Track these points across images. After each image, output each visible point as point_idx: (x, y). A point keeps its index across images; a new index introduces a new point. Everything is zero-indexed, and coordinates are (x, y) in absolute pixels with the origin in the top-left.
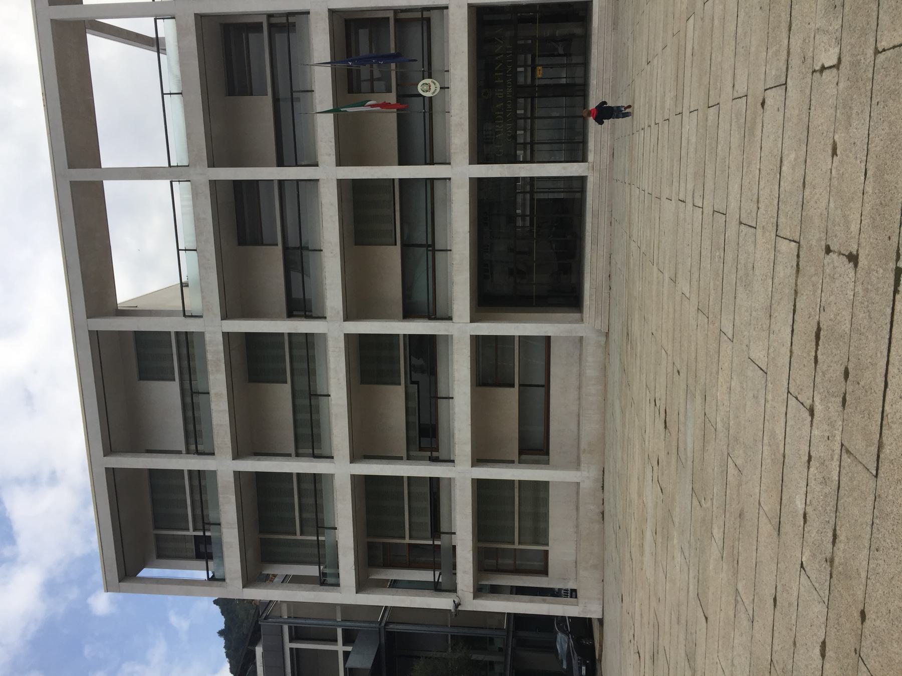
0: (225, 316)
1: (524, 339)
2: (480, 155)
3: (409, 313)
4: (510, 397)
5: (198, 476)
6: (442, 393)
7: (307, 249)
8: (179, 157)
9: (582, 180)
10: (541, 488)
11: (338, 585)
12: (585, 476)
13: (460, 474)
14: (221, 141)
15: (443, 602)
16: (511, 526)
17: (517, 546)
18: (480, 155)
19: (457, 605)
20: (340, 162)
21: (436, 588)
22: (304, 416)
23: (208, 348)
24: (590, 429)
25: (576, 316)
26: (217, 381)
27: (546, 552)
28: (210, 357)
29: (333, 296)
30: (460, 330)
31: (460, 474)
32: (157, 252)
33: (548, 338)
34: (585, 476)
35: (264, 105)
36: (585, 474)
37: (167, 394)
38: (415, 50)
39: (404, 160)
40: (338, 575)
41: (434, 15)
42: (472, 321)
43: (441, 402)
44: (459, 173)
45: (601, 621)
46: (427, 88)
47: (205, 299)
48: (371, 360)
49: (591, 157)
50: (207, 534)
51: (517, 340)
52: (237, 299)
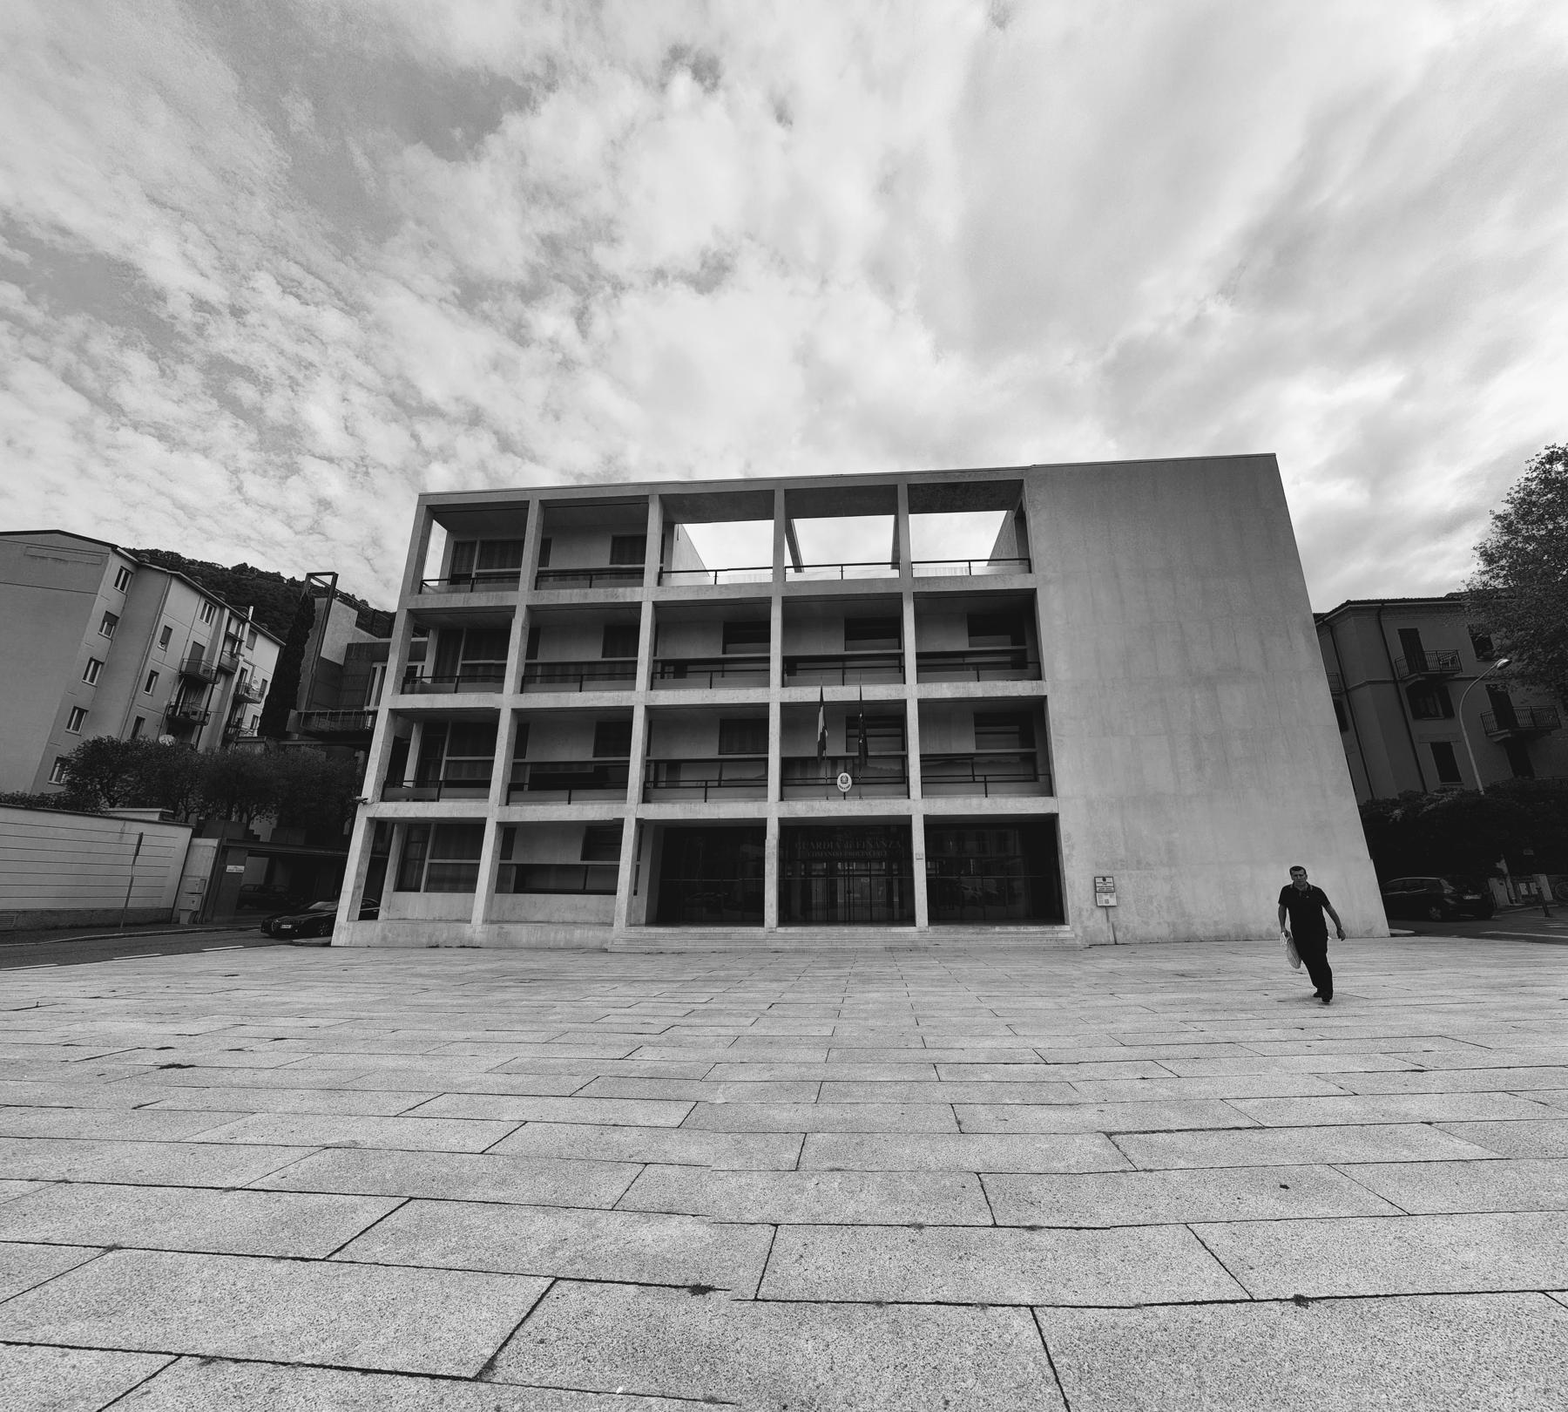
0: (656, 605)
1: (615, 871)
2: (787, 826)
5: (516, 577)
6: (575, 794)
8: (920, 571)
9: (760, 922)
10: (469, 884)
11: (403, 692)
12: (477, 929)
13: (492, 809)
14: (806, 611)
15: (369, 788)
16: (438, 856)
18: (787, 826)
20: (784, 706)
22: (572, 670)
23: (629, 589)
24: (523, 934)
26: (599, 595)
28: (621, 590)
30: (631, 809)
32: (726, 556)
33: (614, 893)
34: (477, 929)
35: (837, 649)
36: (479, 929)
37: (600, 557)
40: (412, 692)
41: (903, 788)
43: (565, 794)
45: (328, 945)
46: (844, 780)
47: (681, 587)
49: (781, 930)
52: (672, 617)
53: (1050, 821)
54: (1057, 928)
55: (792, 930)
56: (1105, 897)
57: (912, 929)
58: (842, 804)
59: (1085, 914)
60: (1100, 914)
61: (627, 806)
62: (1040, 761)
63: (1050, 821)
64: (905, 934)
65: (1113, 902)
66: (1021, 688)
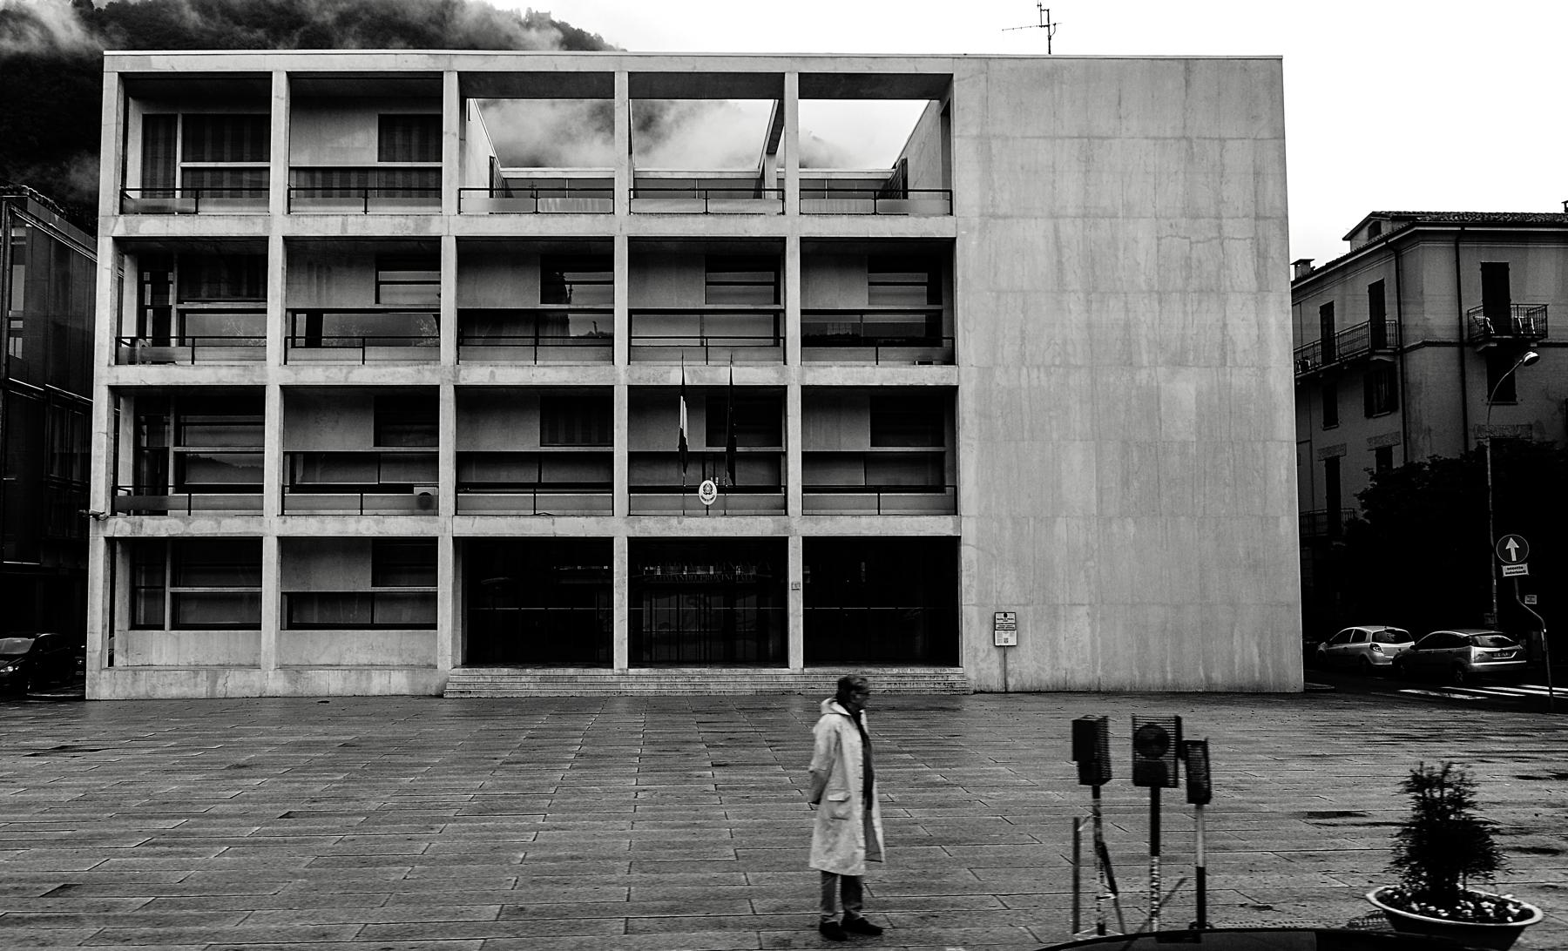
1: (432, 599)
3: (464, 460)
4: (361, 581)
7: (536, 345)
9: (608, 662)
15: (99, 500)
16: (197, 583)
17: (169, 590)
19: (96, 516)
21: (115, 488)
25: (459, 661)
27: (162, 628)
29: (479, 374)
31: (271, 521)
38: (744, 475)
39: (633, 458)
42: (454, 538)
44: (619, 522)
46: (708, 490)
48: (406, 412)
50: (178, 193)
51: (431, 589)
53: (951, 545)
54: (948, 670)
55: (644, 671)
56: (1005, 635)
57: (786, 670)
58: (708, 517)
59: (981, 655)
60: (995, 656)
61: (441, 519)
62: (947, 464)
63: (951, 545)
64: (777, 676)
65: (1012, 642)
66: (931, 375)
